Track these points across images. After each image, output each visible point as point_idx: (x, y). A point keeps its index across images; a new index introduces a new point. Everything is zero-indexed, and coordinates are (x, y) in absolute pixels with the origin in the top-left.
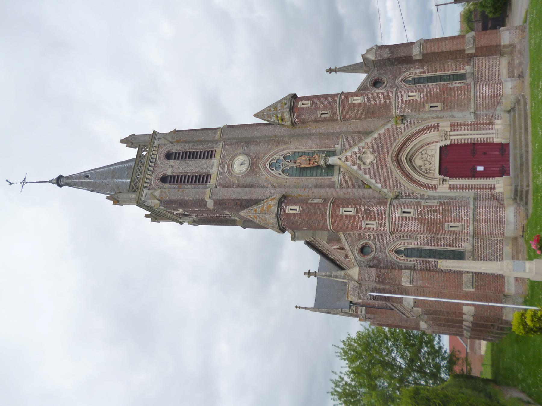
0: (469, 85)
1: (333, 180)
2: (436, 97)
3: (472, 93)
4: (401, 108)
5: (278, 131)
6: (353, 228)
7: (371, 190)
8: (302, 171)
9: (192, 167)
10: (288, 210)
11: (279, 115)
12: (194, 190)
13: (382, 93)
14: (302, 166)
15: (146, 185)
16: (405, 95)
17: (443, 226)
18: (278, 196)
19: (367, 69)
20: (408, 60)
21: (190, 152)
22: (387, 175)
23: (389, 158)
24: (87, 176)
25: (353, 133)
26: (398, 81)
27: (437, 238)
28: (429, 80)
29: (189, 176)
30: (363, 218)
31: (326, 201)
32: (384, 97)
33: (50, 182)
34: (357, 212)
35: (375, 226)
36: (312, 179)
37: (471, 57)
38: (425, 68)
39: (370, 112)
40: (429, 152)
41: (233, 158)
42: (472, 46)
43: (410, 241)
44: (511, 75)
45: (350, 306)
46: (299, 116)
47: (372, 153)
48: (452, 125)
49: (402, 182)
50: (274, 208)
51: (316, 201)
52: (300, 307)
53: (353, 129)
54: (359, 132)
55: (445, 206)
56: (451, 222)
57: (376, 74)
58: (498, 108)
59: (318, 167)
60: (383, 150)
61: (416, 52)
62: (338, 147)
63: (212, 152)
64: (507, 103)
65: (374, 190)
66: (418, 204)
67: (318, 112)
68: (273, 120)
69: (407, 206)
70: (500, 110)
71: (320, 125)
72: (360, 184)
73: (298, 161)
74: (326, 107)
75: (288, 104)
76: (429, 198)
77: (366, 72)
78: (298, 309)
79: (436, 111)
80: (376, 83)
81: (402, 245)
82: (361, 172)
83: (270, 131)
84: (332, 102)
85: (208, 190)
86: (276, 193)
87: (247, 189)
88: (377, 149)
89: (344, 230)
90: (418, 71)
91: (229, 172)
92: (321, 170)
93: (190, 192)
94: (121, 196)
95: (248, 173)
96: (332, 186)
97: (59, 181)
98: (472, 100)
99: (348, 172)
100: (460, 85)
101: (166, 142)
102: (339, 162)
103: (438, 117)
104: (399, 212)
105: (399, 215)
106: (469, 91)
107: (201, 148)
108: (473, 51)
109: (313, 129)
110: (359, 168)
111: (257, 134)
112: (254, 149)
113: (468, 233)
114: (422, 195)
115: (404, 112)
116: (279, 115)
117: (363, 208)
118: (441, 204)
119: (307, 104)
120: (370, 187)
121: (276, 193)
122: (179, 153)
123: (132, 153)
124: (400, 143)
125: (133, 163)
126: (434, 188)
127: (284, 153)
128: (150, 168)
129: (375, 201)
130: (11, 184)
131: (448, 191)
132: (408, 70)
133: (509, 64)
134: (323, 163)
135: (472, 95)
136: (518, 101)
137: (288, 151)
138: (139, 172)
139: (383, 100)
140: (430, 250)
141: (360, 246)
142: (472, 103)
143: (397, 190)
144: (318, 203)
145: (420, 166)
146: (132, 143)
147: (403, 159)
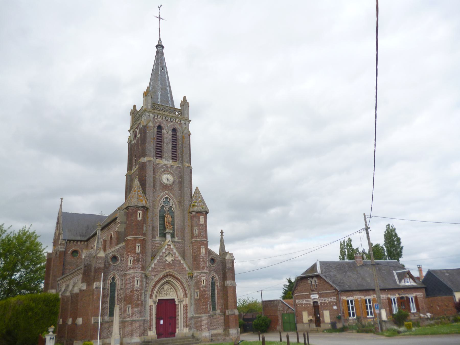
0: (208, 313)
1: (157, 237)
2: (202, 295)
3: (204, 315)
4: (197, 276)
5: (187, 203)
6: (128, 252)
7: (150, 260)
8: (162, 218)
9: (167, 147)
10: (140, 212)
11: (196, 204)
12: (152, 149)
13: (206, 265)
14: (166, 218)
15: (156, 116)
16: (205, 278)
17: (129, 303)
18: (148, 206)
19: (221, 254)
20: (224, 278)
21: (176, 145)
22: (159, 270)
23: (169, 271)
24: (163, 69)
25: (184, 248)
26: (213, 273)
27: (122, 301)
28: (213, 290)
29: (161, 144)
30: (134, 258)
31: (144, 235)
32: (203, 266)
33: (160, 40)
34: (138, 254)
35: (129, 264)
36: (157, 224)
37: (225, 313)
38: (220, 288)
39: (196, 259)
40: (171, 293)
41: (171, 174)
42: (230, 313)
43: (120, 285)
44: (212, 335)
45: (65, 240)
46: (195, 216)
47: (172, 260)
48: (186, 305)
49: (155, 279)
50: (140, 204)
51: (144, 229)
52: (62, 201)
53: (187, 248)
54: (184, 252)
55: (141, 304)
56: (132, 308)
57: (218, 260)
58: (195, 330)
59: (165, 229)
60: (174, 267)
61: (228, 282)
62: (176, 239)
63: (176, 159)
64: (197, 334)
65: (150, 263)
66: (142, 289)
67: (197, 228)
68: (194, 200)
69: (141, 283)
70: (193, 330)
71: (190, 228)
72: (154, 254)
73: (168, 216)
74: (199, 233)
75: (202, 210)
76: (145, 295)
77: (220, 253)
78: (61, 200)
79: (195, 296)
80: (213, 260)
81: (118, 280)
82: (161, 254)
83: (187, 197)
84: (202, 236)
85: (152, 159)
86: (149, 203)
87: (152, 185)
88: (175, 263)
89: (127, 245)
90: (218, 284)
91: (163, 172)
92: (162, 230)
93: (151, 146)
94: (149, 98)
95: (162, 184)
96: (154, 237)
97: (160, 46)
98: (200, 315)
99: (161, 247)
100: (209, 308)
101: (183, 129)
102: (167, 241)
103: (191, 297)
104: (138, 279)
105: (136, 278)
106: (205, 313)
107: (179, 152)
108: (227, 314)
109: (188, 223)
110: (163, 253)
111: (186, 189)
112: (177, 187)
113: (125, 318)
114: (147, 290)
115: (195, 277)
116: (196, 204)
117: (140, 257)
118: (142, 302)
119: (202, 221)
120: (152, 260)
121: (149, 203)
122: (176, 137)
123: (177, 105)
124: (177, 276)
125: (171, 106)
126: (151, 297)
127: (174, 206)
128: (167, 118)
129: (144, 264)
130: (159, 8)
131: (149, 305)
132: (219, 278)
133: (219, 334)
134: (167, 231)
135: (202, 315)
136: (198, 340)
137: (175, 209)
138: (164, 110)
139: (202, 266)
140: (114, 297)
141: (117, 255)
142: (198, 315)
143: (150, 276)
144: (143, 230)
145: (164, 288)
146: (183, 105)
147: (168, 278)
